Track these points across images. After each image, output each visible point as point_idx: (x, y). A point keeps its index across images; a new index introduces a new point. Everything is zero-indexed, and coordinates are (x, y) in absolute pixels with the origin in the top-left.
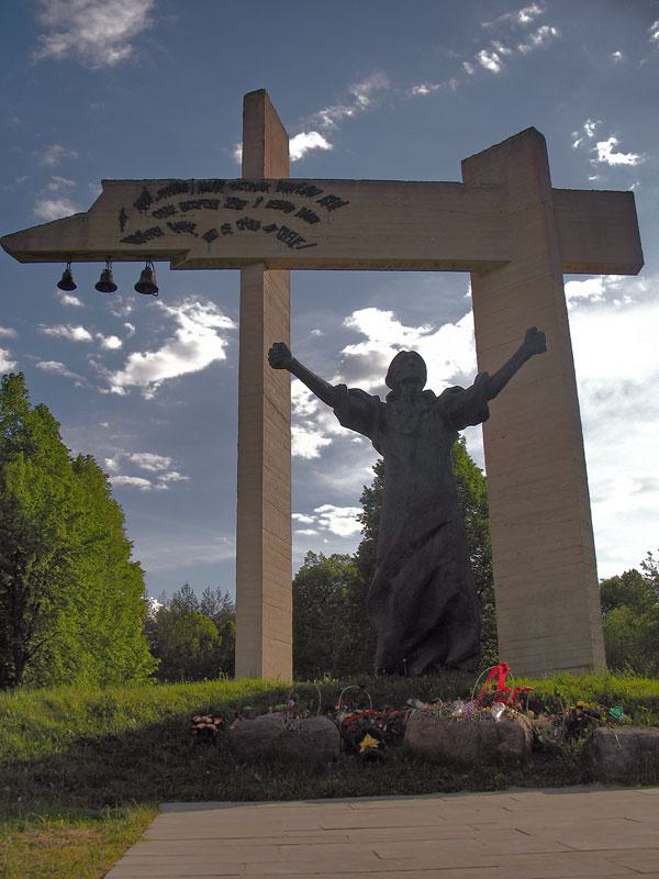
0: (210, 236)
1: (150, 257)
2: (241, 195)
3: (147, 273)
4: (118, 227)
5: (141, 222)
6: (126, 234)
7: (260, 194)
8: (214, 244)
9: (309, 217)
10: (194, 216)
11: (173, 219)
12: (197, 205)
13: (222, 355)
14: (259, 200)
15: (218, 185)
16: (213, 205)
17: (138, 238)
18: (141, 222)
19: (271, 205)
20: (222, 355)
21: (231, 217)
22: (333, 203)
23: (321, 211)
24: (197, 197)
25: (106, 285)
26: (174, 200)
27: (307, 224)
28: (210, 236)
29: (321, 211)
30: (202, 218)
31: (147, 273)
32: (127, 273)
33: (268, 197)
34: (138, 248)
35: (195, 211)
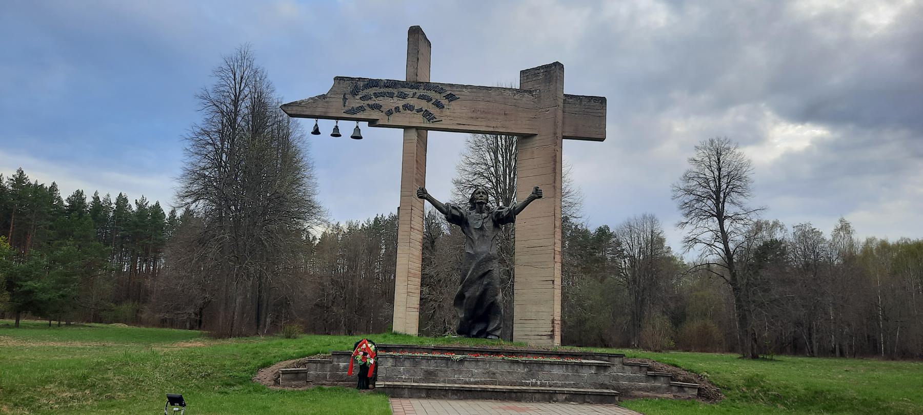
0: (389, 113)
1: (358, 120)
2: (407, 91)
3: (357, 129)
4: (342, 104)
5: (355, 102)
6: (346, 108)
7: (415, 91)
8: (391, 118)
9: (438, 105)
10: (380, 101)
11: (371, 102)
12: (382, 95)
13: (593, 232)
14: (415, 94)
15: (393, 84)
16: (391, 95)
17: (353, 111)
18: (355, 102)
19: (422, 97)
20: (593, 232)
21: (401, 103)
22: (451, 97)
23: (444, 102)
24: (382, 90)
25: (336, 134)
26: (371, 91)
27: (438, 109)
28: (389, 113)
29: (444, 102)
30: (389, 103)
31: (357, 129)
32: (347, 127)
33: (421, 92)
34: (351, 115)
35: (381, 98)
